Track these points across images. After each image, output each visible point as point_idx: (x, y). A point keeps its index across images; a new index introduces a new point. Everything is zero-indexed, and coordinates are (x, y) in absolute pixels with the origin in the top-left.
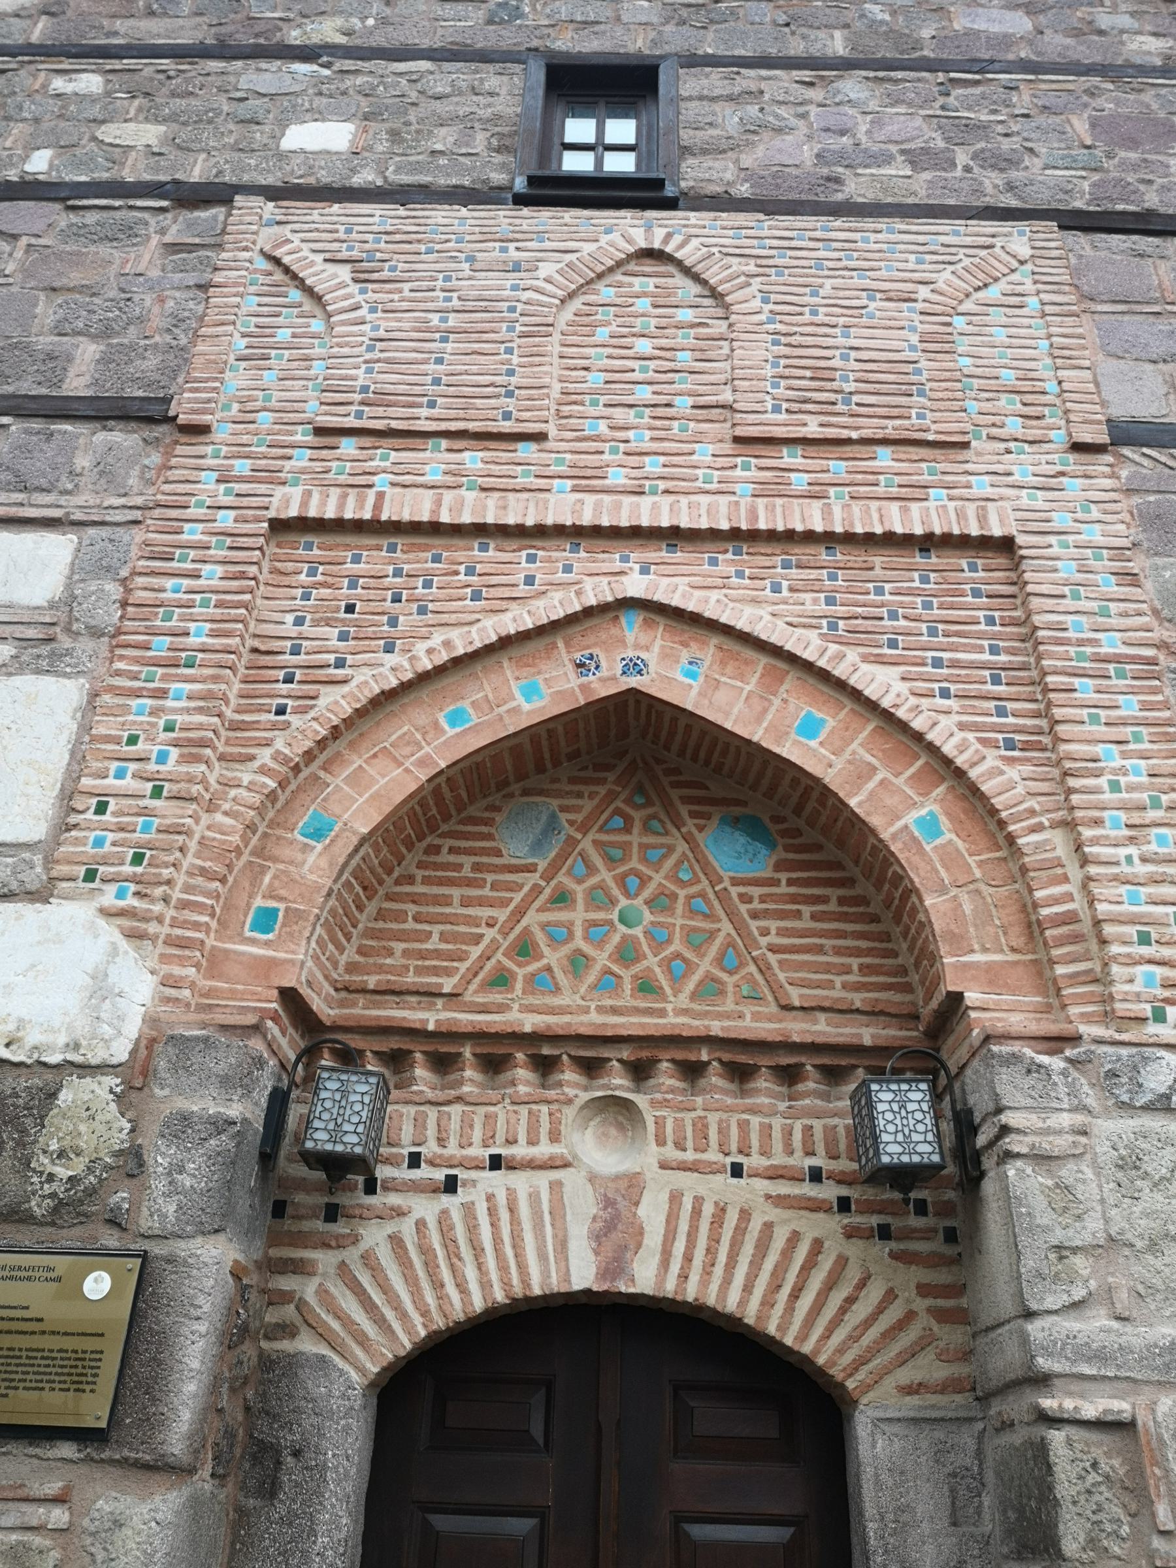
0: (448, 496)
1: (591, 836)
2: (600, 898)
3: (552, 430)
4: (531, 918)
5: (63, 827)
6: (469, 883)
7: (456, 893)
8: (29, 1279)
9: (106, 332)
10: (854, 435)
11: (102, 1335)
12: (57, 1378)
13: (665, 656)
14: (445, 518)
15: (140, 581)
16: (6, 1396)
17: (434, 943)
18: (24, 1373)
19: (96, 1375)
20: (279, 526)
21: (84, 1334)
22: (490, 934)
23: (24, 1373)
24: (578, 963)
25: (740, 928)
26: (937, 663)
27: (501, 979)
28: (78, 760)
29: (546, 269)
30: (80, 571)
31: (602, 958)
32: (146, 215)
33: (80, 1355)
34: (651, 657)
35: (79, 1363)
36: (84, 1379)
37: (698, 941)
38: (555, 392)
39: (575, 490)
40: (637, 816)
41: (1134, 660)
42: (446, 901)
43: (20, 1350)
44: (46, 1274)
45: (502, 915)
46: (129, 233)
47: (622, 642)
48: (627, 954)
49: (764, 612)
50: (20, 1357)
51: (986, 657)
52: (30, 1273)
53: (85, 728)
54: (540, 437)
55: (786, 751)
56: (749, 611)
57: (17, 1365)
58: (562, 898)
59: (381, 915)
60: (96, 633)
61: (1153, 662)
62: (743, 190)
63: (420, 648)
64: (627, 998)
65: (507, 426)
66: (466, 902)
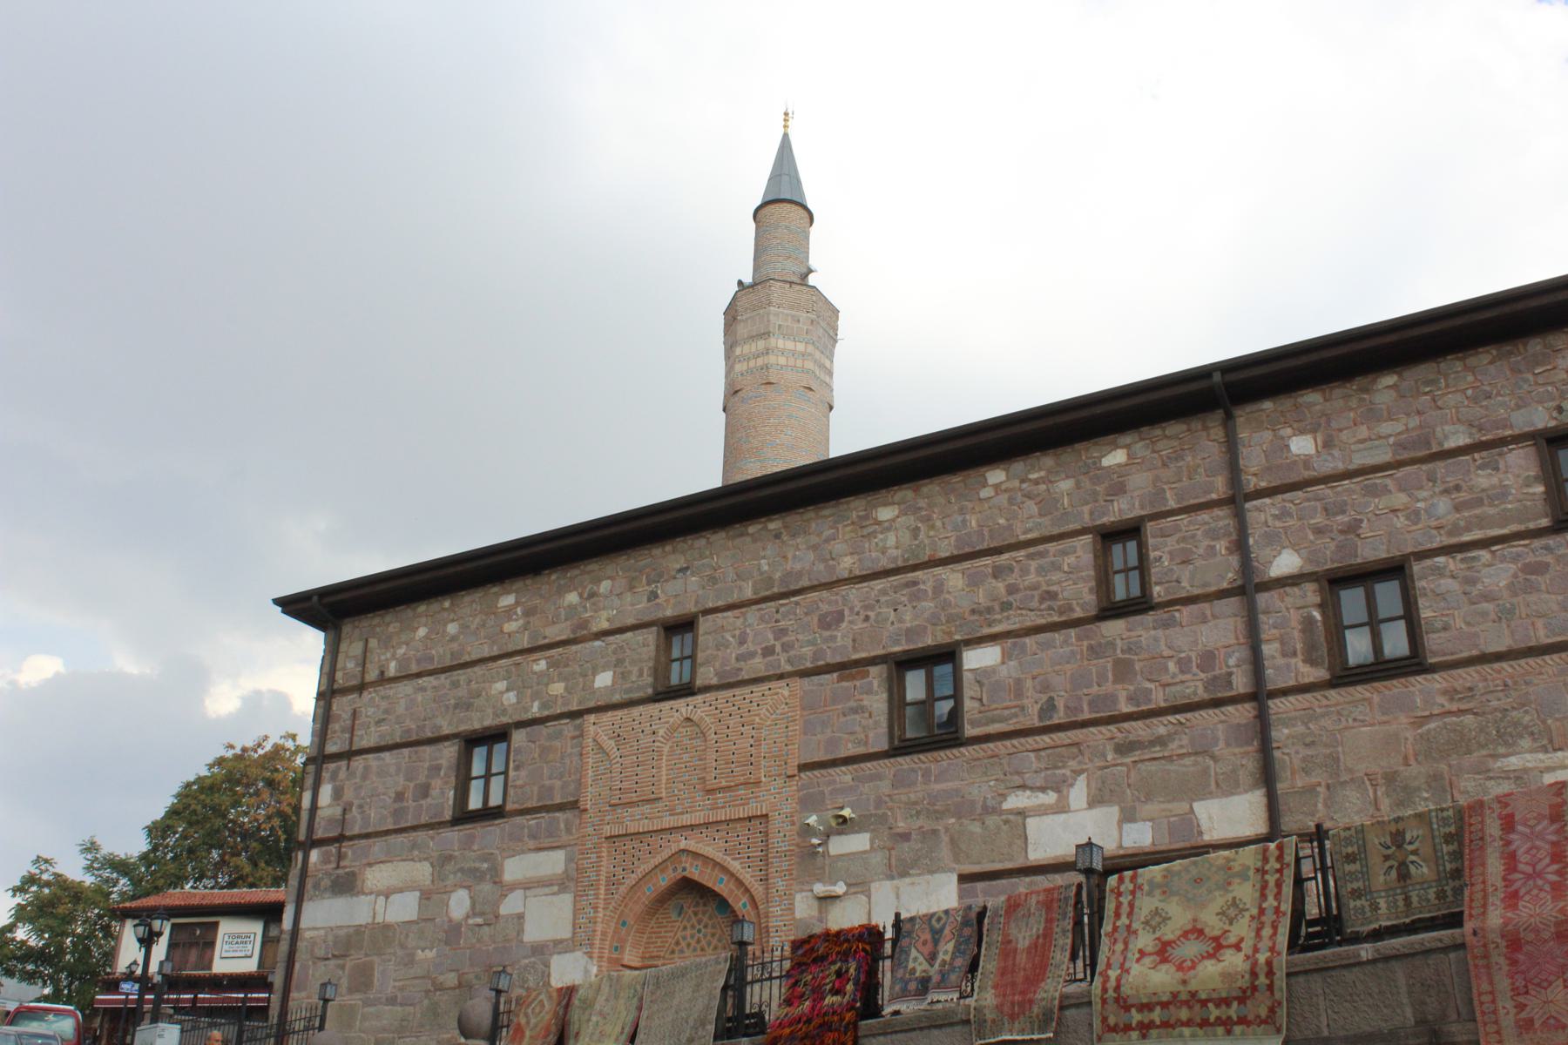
0: (641, 823)
1: (692, 909)
2: (693, 927)
3: (664, 795)
4: (679, 934)
5: (574, 933)
6: (666, 927)
7: (663, 930)
9: (561, 777)
10: (732, 784)
13: (691, 865)
14: (641, 830)
15: (580, 862)
17: (659, 944)
20: (606, 838)
22: (670, 940)
24: (689, 945)
25: (722, 930)
26: (749, 857)
27: (673, 952)
28: (574, 915)
29: (661, 732)
30: (569, 860)
31: (693, 942)
32: (563, 727)
34: (688, 865)
37: (713, 935)
38: (664, 781)
39: (670, 815)
40: (701, 901)
41: (790, 851)
42: (660, 932)
45: (672, 934)
46: (558, 735)
47: (681, 862)
48: (698, 941)
49: (710, 849)
51: (760, 853)
53: (575, 906)
54: (661, 798)
55: (716, 889)
56: (707, 848)
58: (685, 928)
59: (648, 938)
60: (572, 879)
61: (793, 850)
62: (715, 681)
63: (639, 871)
64: (699, 952)
65: (653, 796)
66: (666, 932)
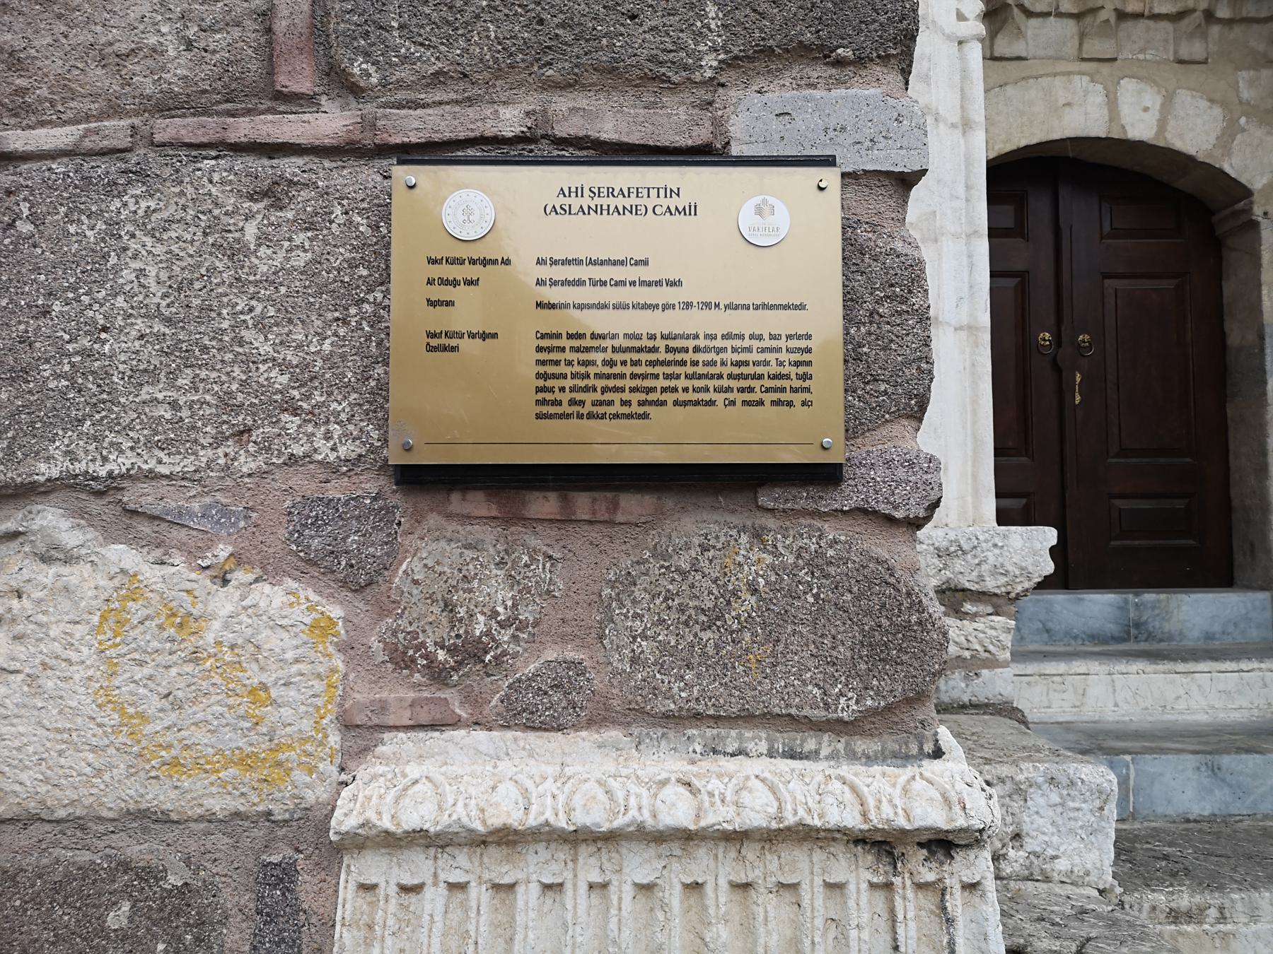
8: (634, 210)
11: (801, 307)
12: (734, 384)
16: (645, 416)
18: (668, 377)
19: (805, 377)
21: (765, 306)
23: (668, 377)
33: (767, 343)
35: (771, 357)
36: (785, 383)
43: (652, 337)
44: (665, 202)
50: (654, 350)
52: (633, 200)
57: (652, 363)
